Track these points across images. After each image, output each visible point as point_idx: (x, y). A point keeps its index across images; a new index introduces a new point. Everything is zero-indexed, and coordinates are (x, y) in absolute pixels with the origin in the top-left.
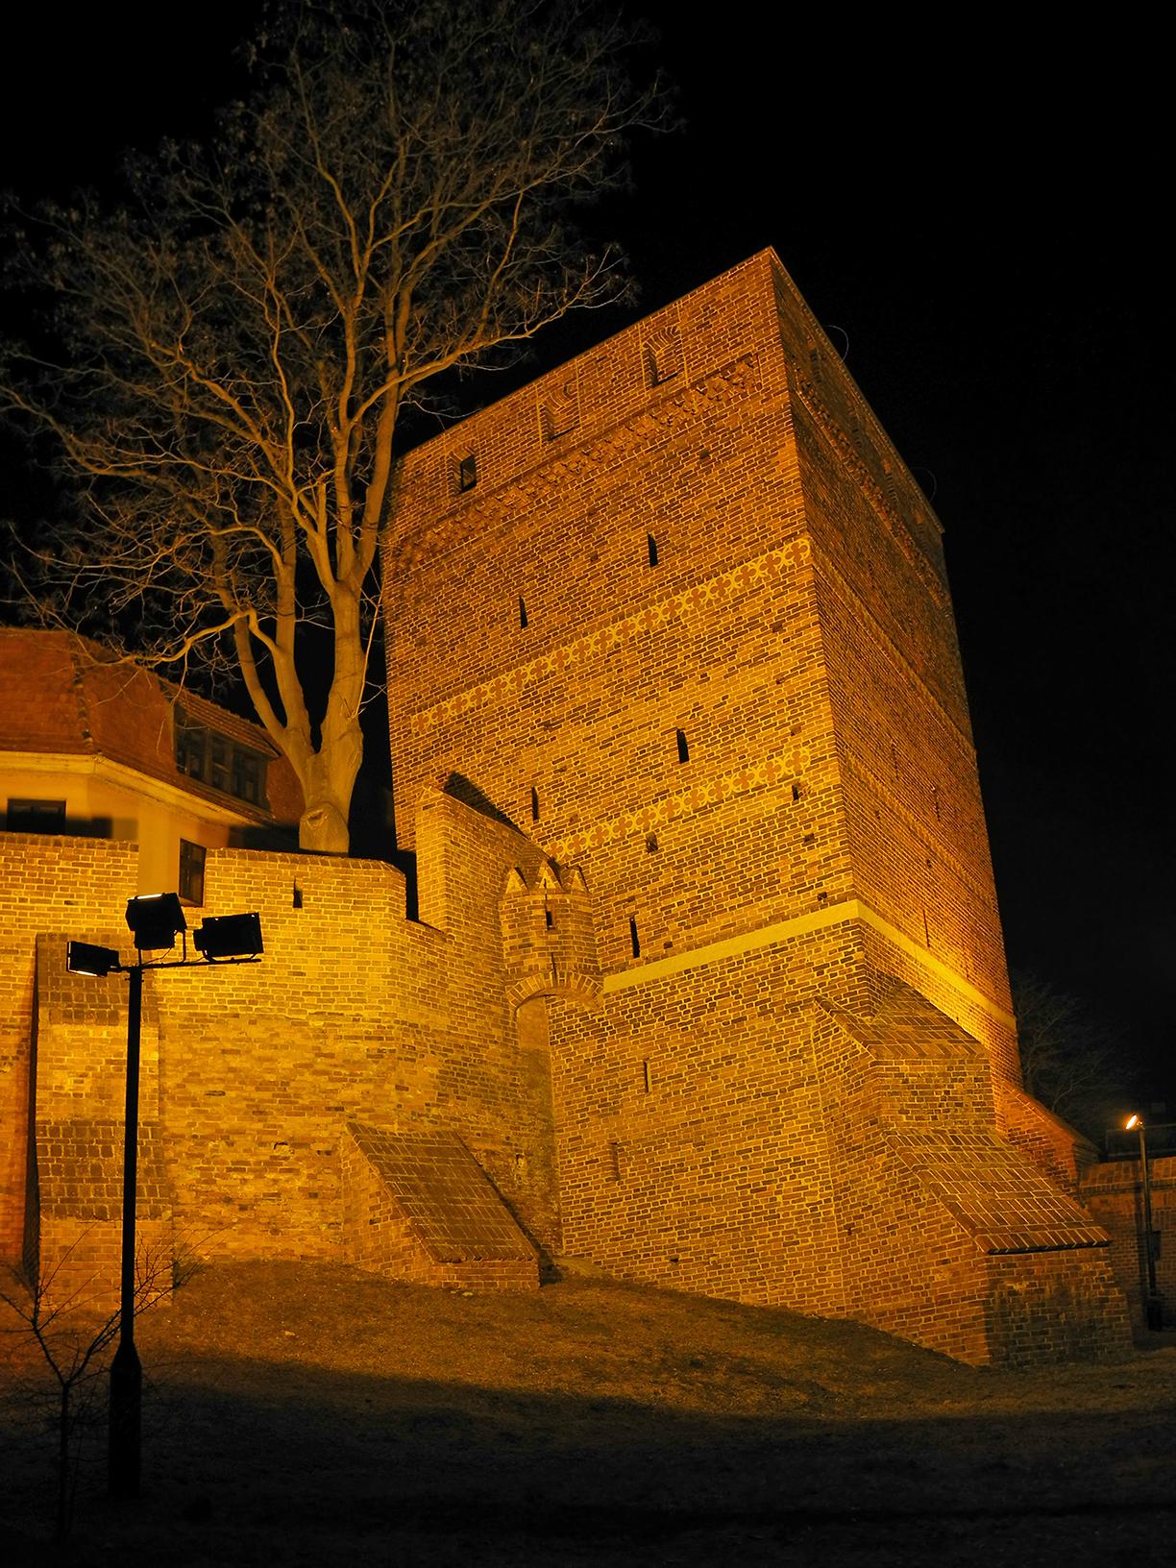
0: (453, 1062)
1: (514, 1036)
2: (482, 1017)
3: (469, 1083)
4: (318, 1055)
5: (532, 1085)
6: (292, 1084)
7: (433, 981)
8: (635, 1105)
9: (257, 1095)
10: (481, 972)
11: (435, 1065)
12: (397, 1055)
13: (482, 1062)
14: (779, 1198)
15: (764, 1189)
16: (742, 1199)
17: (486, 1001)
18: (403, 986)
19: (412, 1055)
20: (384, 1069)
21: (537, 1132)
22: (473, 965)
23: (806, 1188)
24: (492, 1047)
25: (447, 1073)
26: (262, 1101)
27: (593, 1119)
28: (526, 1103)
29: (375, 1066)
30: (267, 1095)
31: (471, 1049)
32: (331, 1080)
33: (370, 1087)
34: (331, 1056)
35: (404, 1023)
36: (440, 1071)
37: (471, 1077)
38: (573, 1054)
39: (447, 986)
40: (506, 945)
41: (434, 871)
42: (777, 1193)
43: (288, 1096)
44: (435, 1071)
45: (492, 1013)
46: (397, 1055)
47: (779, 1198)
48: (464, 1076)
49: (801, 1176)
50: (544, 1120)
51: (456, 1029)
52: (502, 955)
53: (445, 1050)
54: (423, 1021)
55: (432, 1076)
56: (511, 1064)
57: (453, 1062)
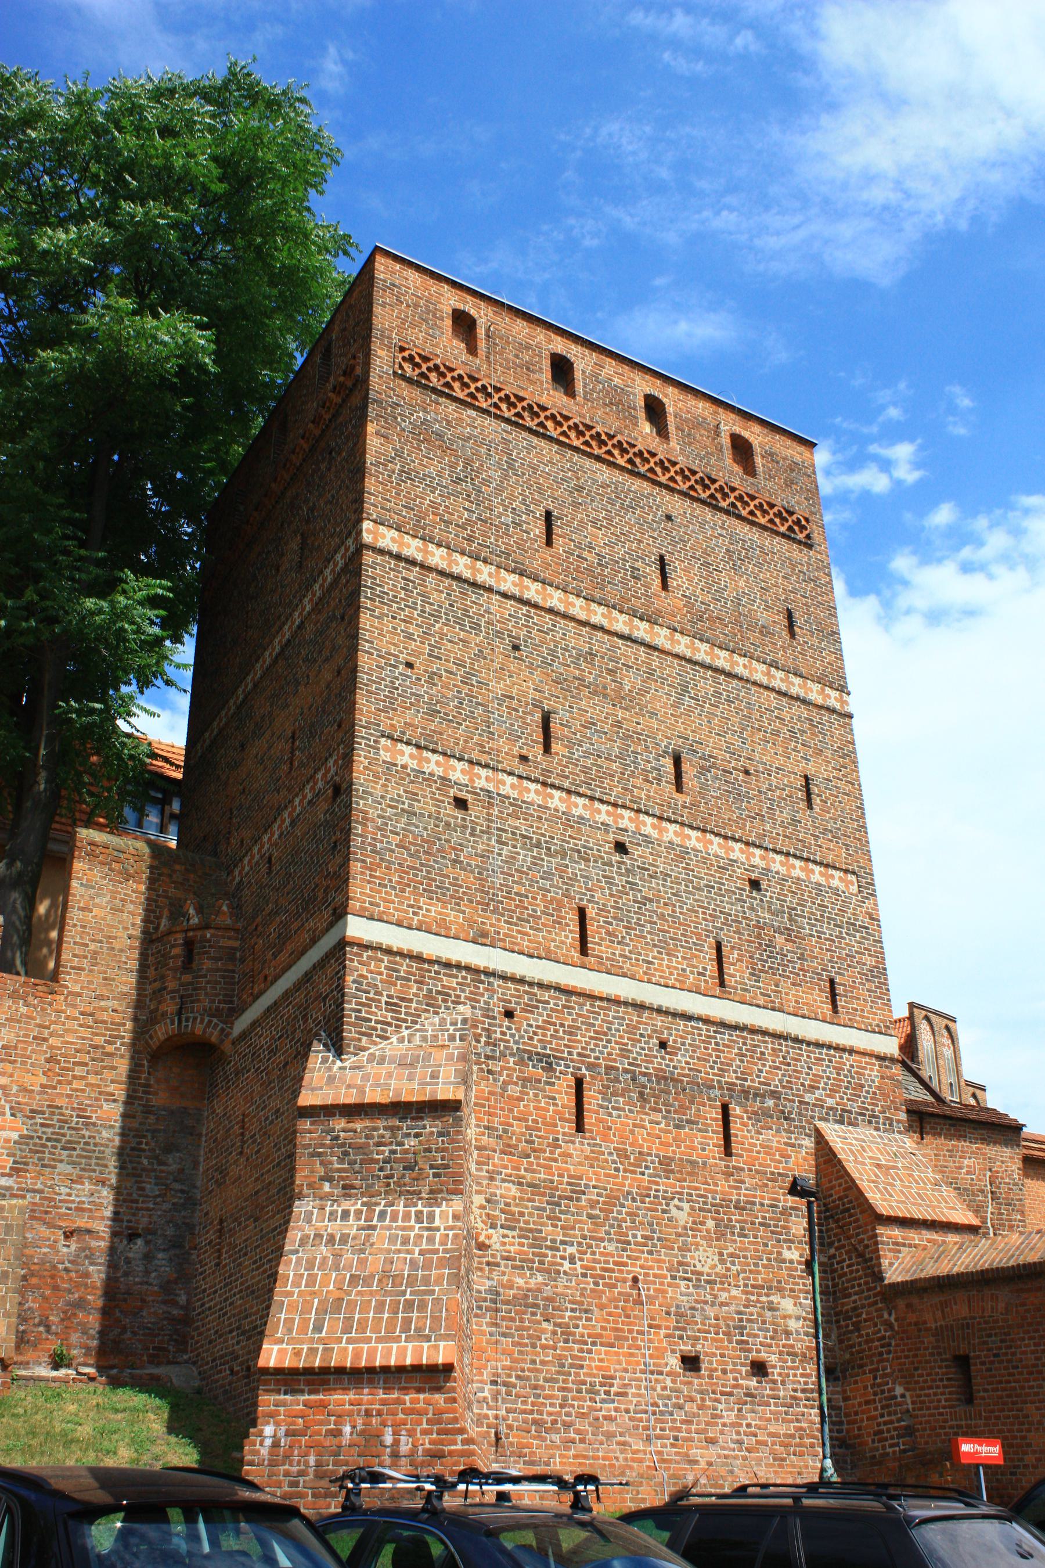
1: (148, 1093)
3: (64, 1148)
5: (168, 1149)
7: (26, 1036)
13: (87, 1124)
21: (166, 1206)
22: (91, 1015)
25: (32, 1138)
28: (155, 1170)
31: (73, 1109)
36: (21, 1136)
37: (69, 1142)
44: (15, 1136)
48: (58, 1141)
50: (182, 1191)
51: (55, 1088)
53: (32, 1111)
56: (136, 1125)
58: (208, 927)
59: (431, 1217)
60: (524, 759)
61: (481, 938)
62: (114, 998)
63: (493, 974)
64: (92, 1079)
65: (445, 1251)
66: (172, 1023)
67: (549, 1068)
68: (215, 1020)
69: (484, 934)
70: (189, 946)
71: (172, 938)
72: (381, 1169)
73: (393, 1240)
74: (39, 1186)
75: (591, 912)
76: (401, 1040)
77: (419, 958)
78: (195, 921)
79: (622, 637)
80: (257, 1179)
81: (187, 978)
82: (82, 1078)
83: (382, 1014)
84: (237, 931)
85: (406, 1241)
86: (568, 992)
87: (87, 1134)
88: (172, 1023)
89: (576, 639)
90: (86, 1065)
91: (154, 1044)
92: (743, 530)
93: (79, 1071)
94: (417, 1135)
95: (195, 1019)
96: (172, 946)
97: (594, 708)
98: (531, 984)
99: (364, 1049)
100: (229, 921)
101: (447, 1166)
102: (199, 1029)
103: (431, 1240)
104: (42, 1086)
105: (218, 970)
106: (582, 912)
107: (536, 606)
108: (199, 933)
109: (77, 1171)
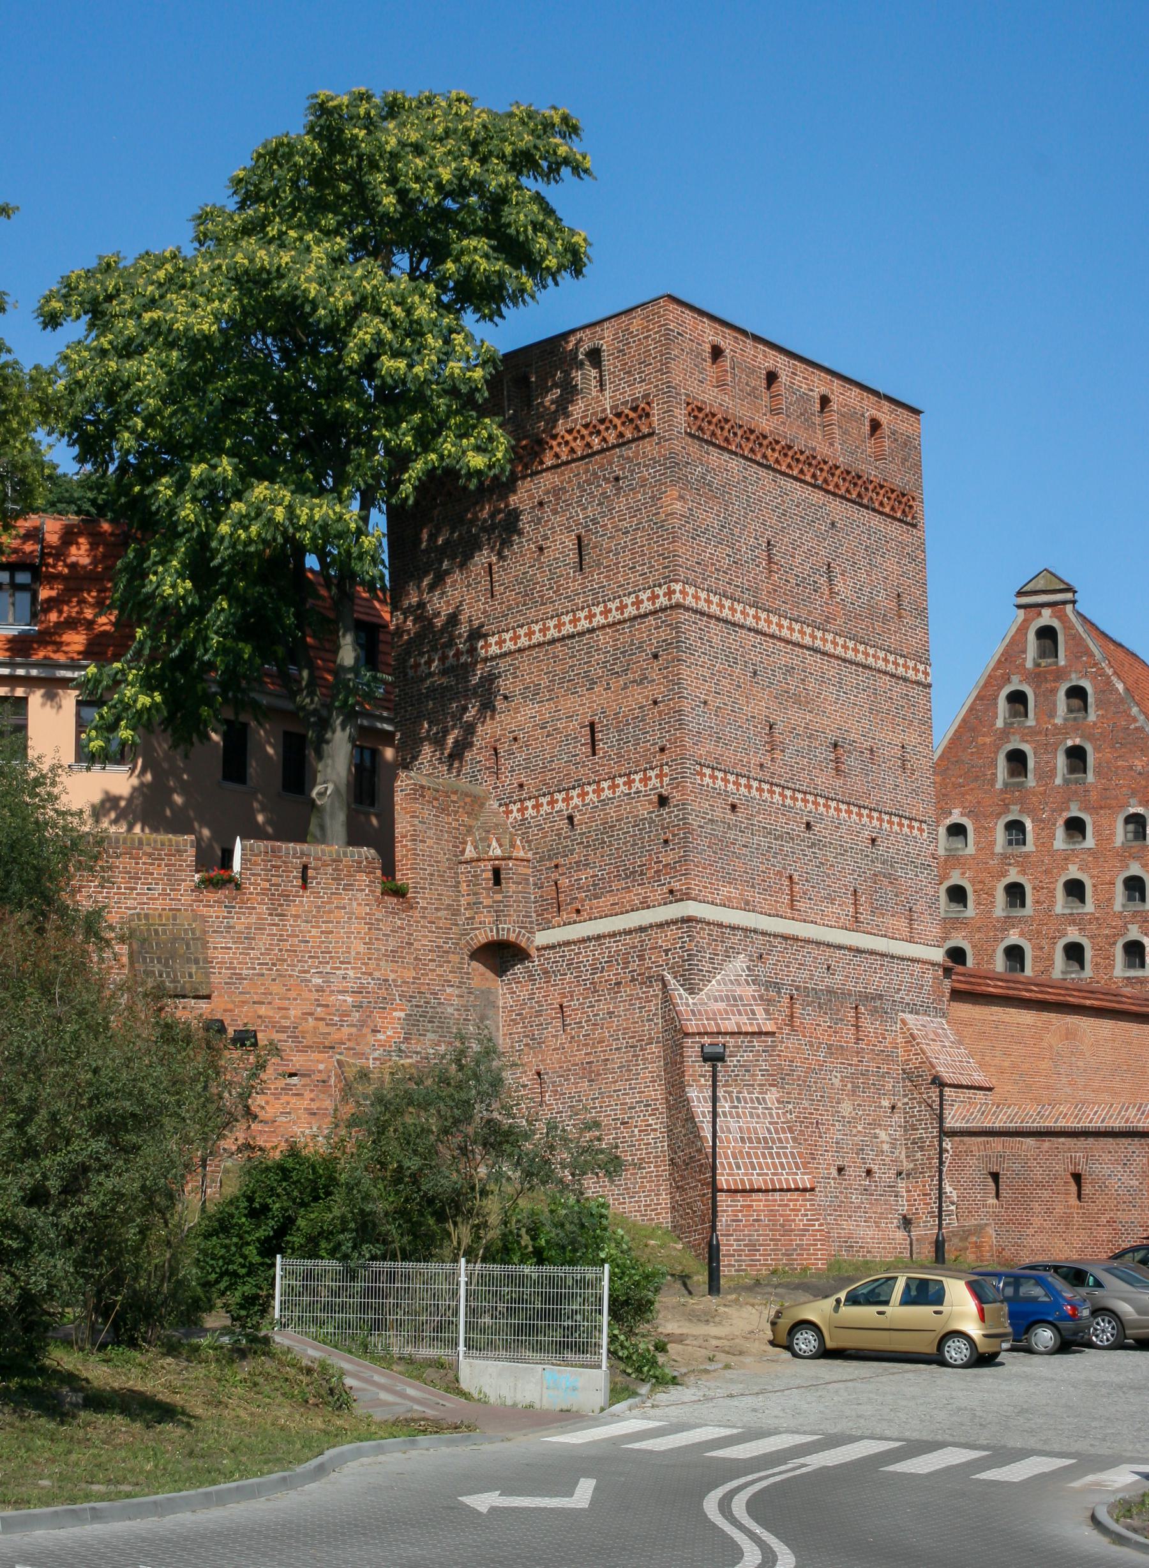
0: (417, 1006)
2: (441, 966)
3: (430, 1022)
4: (318, 1005)
6: (300, 1028)
8: (552, 1043)
9: (276, 1036)
10: (441, 928)
11: (402, 1010)
12: (372, 1005)
13: (440, 1003)
14: (636, 1132)
15: (627, 1123)
16: (615, 1129)
17: (444, 952)
18: (379, 950)
19: (385, 1002)
20: (364, 1018)
23: (651, 1125)
24: (449, 990)
25: (411, 1015)
26: (280, 1041)
27: (526, 1049)
29: (357, 1014)
30: (283, 1036)
32: (327, 1025)
33: (354, 1030)
34: (327, 1006)
35: (379, 979)
38: (515, 993)
39: (412, 944)
40: (463, 902)
41: (406, 846)
42: (636, 1127)
43: (297, 1037)
44: (402, 1015)
45: (449, 962)
46: (372, 1005)
47: (636, 1130)
49: (650, 1115)
52: (459, 910)
54: (392, 976)
55: (399, 1019)
57: (417, 1006)
58: (510, 858)
59: (764, 1099)
60: (761, 765)
61: (747, 906)
62: (445, 909)
63: (755, 931)
64: (439, 971)
65: (783, 1123)
66: (492, 931)
67: (779, 992)
68: (523, 931)
69: (747, 903)
70: (497, 872)
71: (482, 864)
72: (733, 1071)
73: (751, 1114)
74: (419, 1049)
75: (796, 878)
76: (718, 982)
77: (720, 925)
78: (498, 852)
79: (809, 649)
80: (586, 1054)
81: (499, 897)
82: (434, 970)
83: (707, 967)
84: (528, 861)
85: (758, 1117)
86: (785, 938)
87: (439, 1010)
88: (492, 931)
89: (784, 656)
90: (434, 961)
91: (475, 944)
92: (876, 520)
93: (432, 966)
94: (751, 1051)
95: (509, 929)
96: (483, 871)
97: (796, 716)
98: (770, 935)
99: (701, 990)
100: (521, 854)
101: (767, 1070)
102: (512, 937)
103: (771, 1115)
104: (414, 978)
105: (520, 892)
106: (791, 877)
107: (765, 634)
108: (503, 863)
109: (437, 1038)
